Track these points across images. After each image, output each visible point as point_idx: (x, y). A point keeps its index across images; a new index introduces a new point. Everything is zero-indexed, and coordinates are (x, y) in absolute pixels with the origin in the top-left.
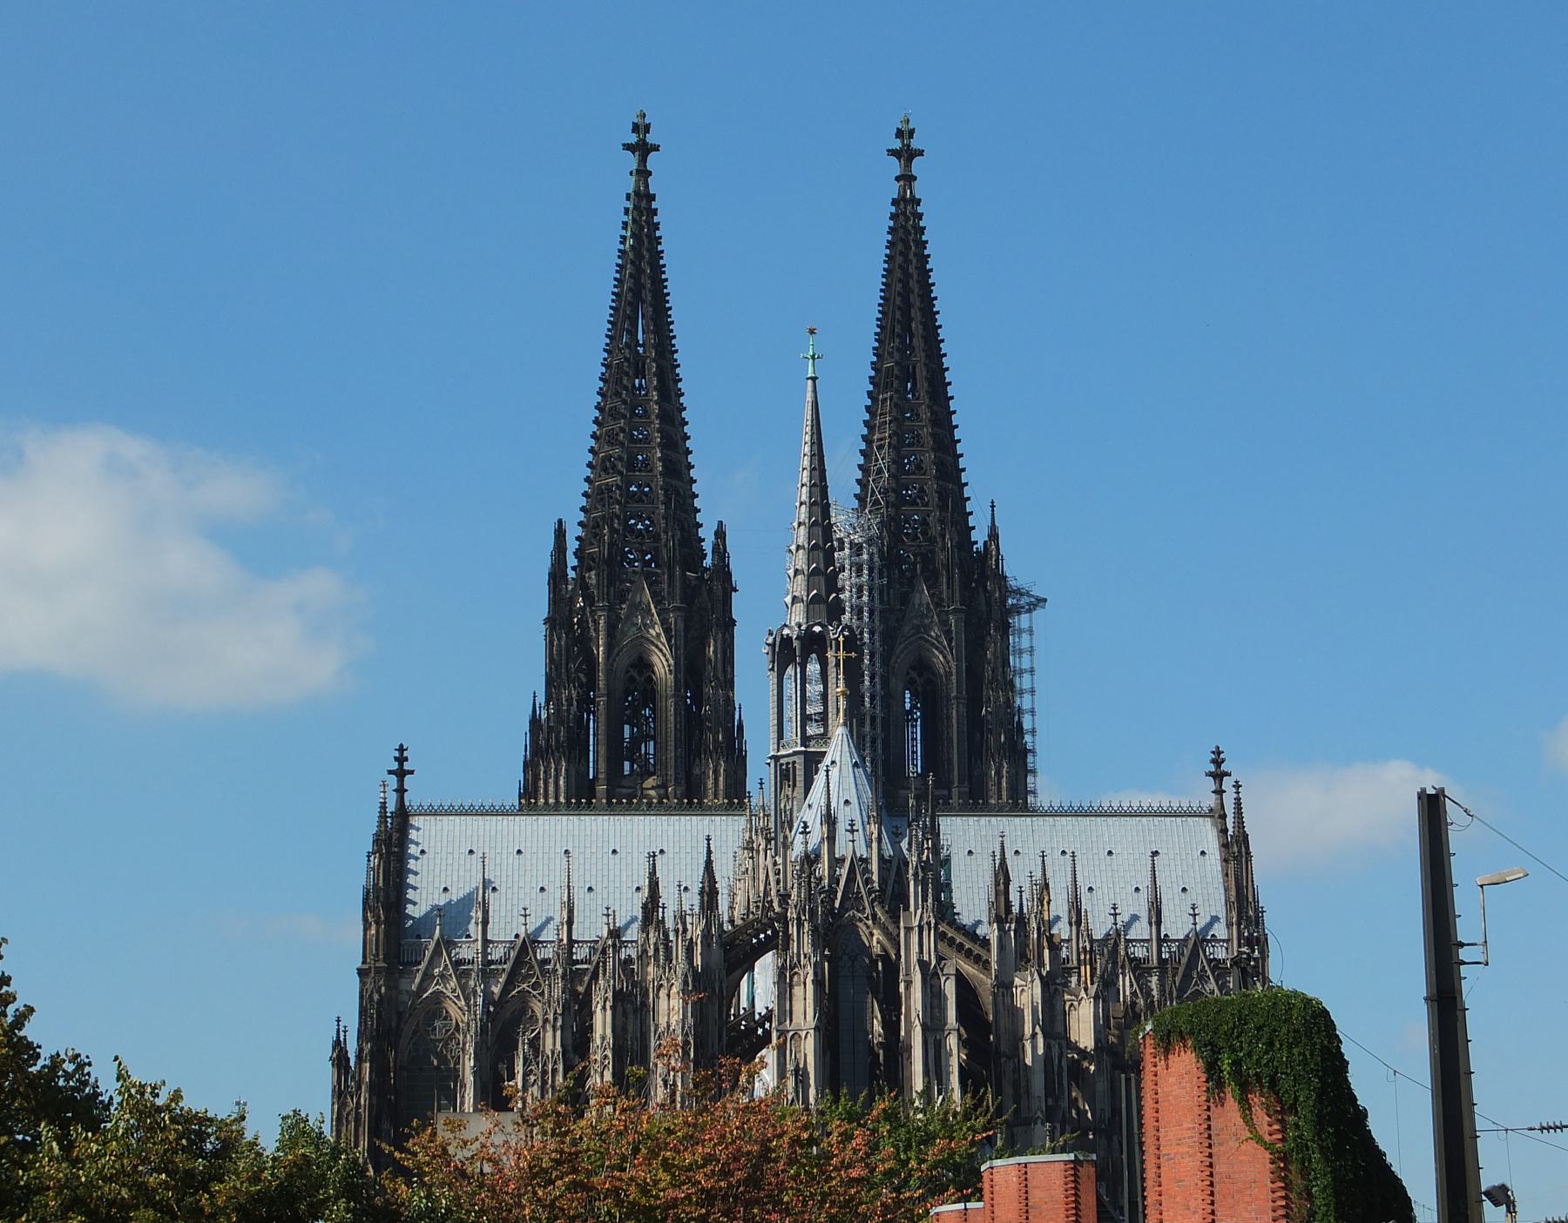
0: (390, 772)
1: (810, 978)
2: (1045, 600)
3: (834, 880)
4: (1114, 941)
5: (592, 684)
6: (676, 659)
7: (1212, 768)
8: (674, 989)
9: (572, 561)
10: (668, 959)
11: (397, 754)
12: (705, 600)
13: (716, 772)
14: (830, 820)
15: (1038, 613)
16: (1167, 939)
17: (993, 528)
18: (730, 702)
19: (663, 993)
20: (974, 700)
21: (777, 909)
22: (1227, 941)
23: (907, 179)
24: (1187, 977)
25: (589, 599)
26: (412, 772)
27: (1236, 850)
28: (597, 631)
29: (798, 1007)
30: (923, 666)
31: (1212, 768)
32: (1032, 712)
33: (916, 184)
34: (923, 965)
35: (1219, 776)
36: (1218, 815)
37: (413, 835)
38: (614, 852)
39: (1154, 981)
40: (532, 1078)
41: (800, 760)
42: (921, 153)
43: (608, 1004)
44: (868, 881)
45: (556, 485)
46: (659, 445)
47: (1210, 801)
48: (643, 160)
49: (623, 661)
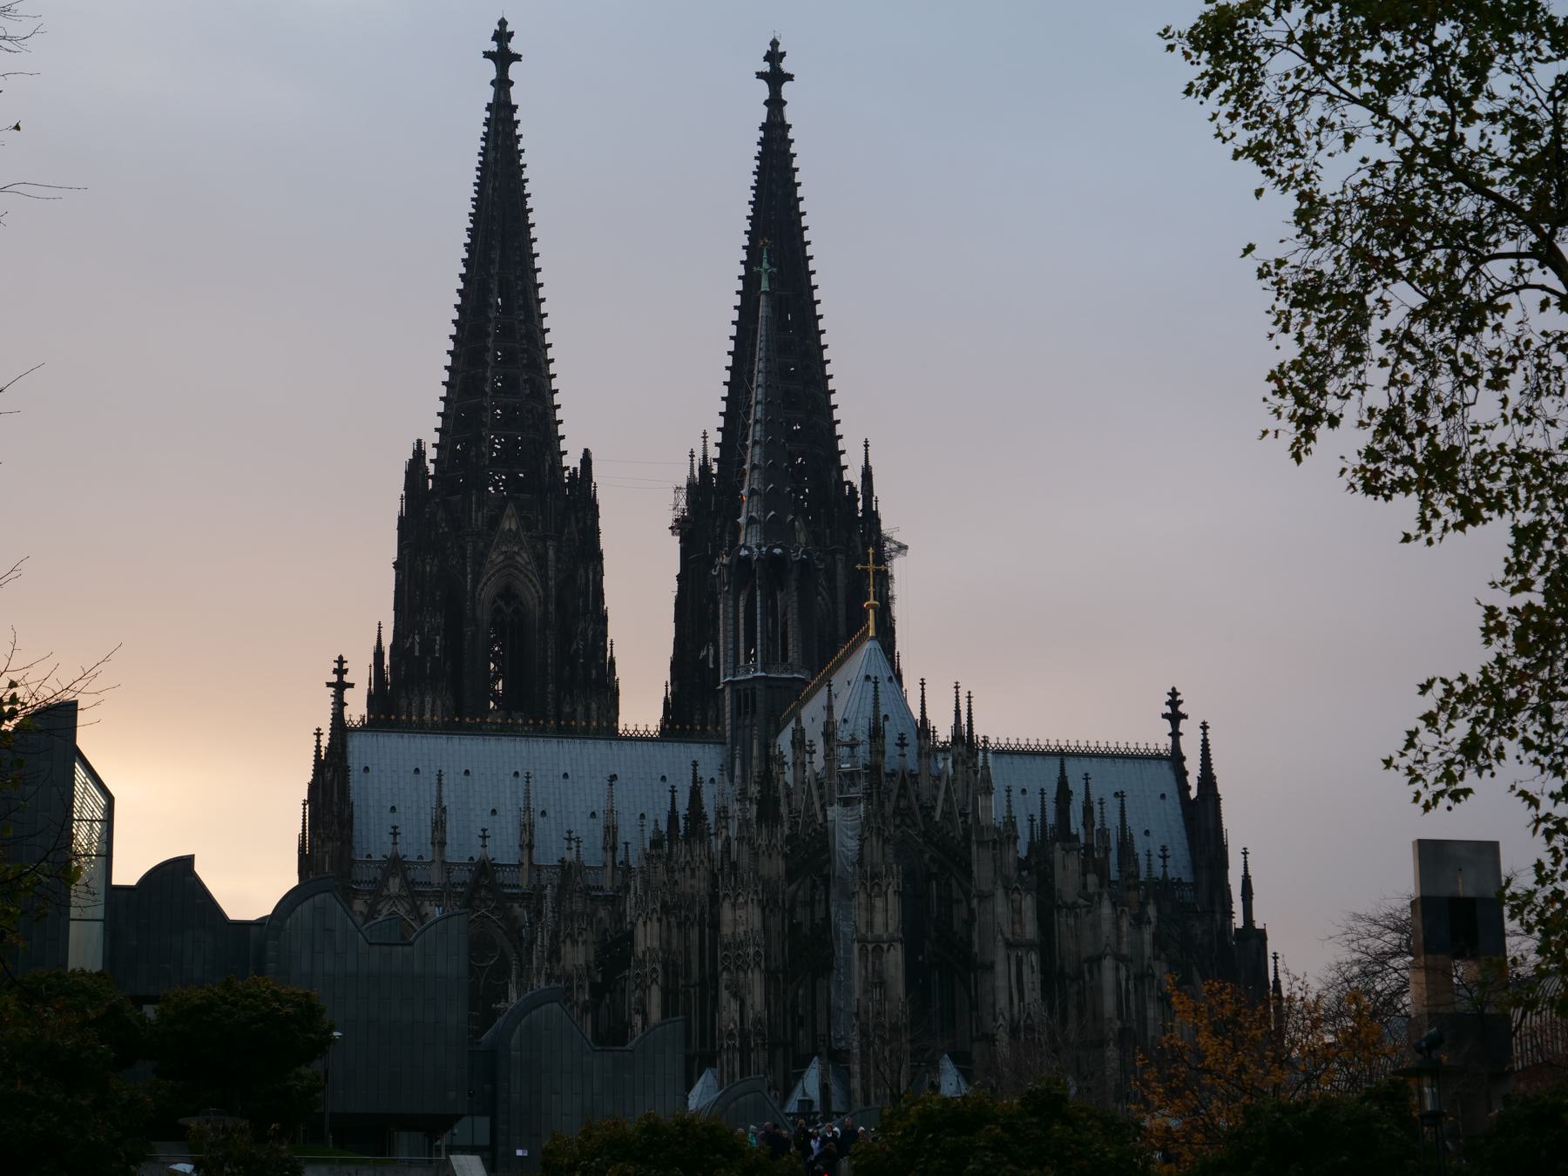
0: (329, 685)
2: (906, 547)
7: (1168, 710)
8: (741, 899)
11: (336, 666)
19: (726, 905)
31: (1168, 710)
35: (1175, 717)
38: (566, 775)
43: (655, 917)
47: (1164, 743)
49: (488, 591)
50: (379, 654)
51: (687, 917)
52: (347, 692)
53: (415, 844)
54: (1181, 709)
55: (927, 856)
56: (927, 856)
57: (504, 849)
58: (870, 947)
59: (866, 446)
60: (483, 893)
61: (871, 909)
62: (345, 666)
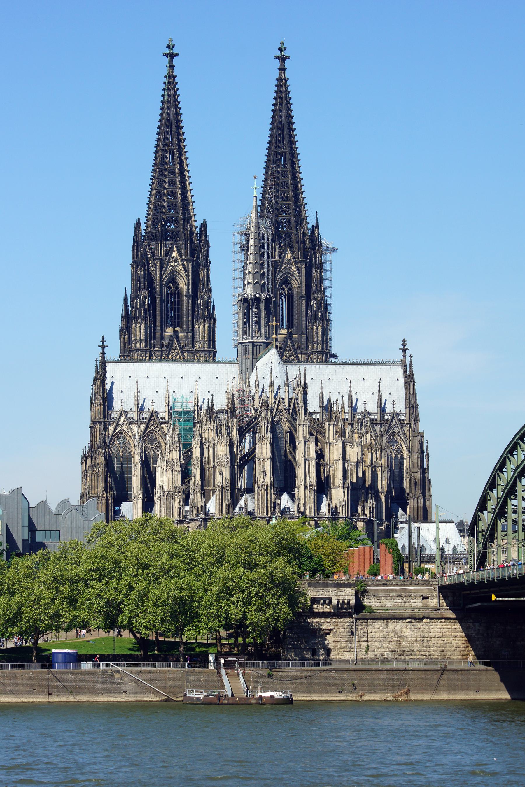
0: (99, 346)
1: (269, 442)
6: (188, 280)
8: (223, 444)
9: (143, 238)
10: (221, 433)
11: (102, 340)
12: (198, 250)
13: (204, 327)
15: (334, 254)
17: (317, 223)
19: (219, 445)
20: (308, 298)
21: (254, 414)
22: (405, 414)
23: (282, 69)
26: (107, 346)
27: (409, 379)
32: (331, 296)
33: (286, 71)
35: (404, 350)
36: (404, 364)
40: (169, 467)
41: (251, 345)
42: (289, 57)
44: (284, 406)
45: (135, 204)
46: (180, 188)
50: (126, 300)
51: (209, 445)
52: (106, 349)
53: (130, 405)
54: (406, 347)
55: (287, 425)
56: (287, 425)
57: (161, 407)
58: (261, 460)
59: (317, 214)
60: (153, 422)
61: (262, 448)
62: (105, 340)
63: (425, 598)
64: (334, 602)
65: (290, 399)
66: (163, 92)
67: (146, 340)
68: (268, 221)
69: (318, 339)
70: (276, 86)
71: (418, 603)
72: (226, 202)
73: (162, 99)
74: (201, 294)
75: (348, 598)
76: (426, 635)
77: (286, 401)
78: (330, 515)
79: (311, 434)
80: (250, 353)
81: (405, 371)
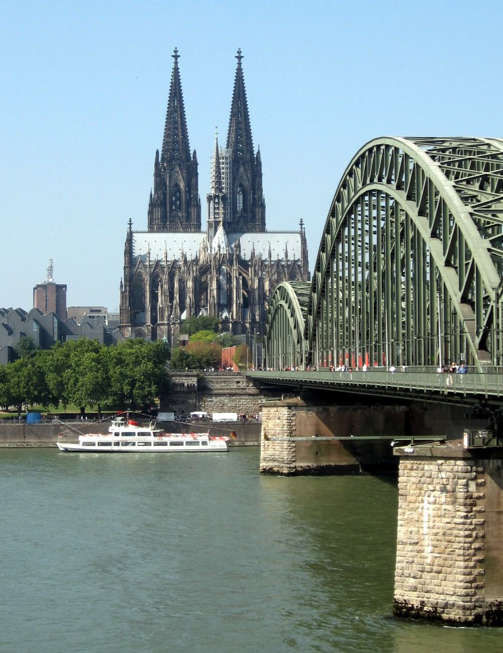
3: (220, 258)
4: (279, 261)
5: (166, 189)
6: (185, 184)
9: (160, 160)
10: (189, 274)
14: (219, 247)
16: (289, 261)
17: (259, 151)
18: (197, 194)
20: (254, 194)
24: (293, 268)
25: (165, 169)
28: (167, 177)
29: (213, 284)
30: (241, 185)
34: (236, 277)
35: (301, 225)
37: (133, 238)
39: (286, 269)
41: (213, 222)
45: (156, 141)
48: (176, 60)
49: (173, 184)
54: (303, 223)
63: (238, 382)
64: (186, 385)
65: (229, 254)
66: (172, 78)
67: (161, 218)
68: (231, 150)
69: (259, 217)
70: (236, 73)
71: (235, 386)
72: (208, 139)
73: (171, 81)
74: (192, 191)
75: (193, 383)
76: (238, 403)
77: (228, 255)
78: (250, 321)
79: (240, 274)
80: (214, 226)
81: (302, 237)
